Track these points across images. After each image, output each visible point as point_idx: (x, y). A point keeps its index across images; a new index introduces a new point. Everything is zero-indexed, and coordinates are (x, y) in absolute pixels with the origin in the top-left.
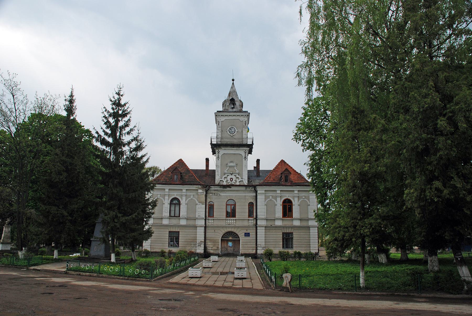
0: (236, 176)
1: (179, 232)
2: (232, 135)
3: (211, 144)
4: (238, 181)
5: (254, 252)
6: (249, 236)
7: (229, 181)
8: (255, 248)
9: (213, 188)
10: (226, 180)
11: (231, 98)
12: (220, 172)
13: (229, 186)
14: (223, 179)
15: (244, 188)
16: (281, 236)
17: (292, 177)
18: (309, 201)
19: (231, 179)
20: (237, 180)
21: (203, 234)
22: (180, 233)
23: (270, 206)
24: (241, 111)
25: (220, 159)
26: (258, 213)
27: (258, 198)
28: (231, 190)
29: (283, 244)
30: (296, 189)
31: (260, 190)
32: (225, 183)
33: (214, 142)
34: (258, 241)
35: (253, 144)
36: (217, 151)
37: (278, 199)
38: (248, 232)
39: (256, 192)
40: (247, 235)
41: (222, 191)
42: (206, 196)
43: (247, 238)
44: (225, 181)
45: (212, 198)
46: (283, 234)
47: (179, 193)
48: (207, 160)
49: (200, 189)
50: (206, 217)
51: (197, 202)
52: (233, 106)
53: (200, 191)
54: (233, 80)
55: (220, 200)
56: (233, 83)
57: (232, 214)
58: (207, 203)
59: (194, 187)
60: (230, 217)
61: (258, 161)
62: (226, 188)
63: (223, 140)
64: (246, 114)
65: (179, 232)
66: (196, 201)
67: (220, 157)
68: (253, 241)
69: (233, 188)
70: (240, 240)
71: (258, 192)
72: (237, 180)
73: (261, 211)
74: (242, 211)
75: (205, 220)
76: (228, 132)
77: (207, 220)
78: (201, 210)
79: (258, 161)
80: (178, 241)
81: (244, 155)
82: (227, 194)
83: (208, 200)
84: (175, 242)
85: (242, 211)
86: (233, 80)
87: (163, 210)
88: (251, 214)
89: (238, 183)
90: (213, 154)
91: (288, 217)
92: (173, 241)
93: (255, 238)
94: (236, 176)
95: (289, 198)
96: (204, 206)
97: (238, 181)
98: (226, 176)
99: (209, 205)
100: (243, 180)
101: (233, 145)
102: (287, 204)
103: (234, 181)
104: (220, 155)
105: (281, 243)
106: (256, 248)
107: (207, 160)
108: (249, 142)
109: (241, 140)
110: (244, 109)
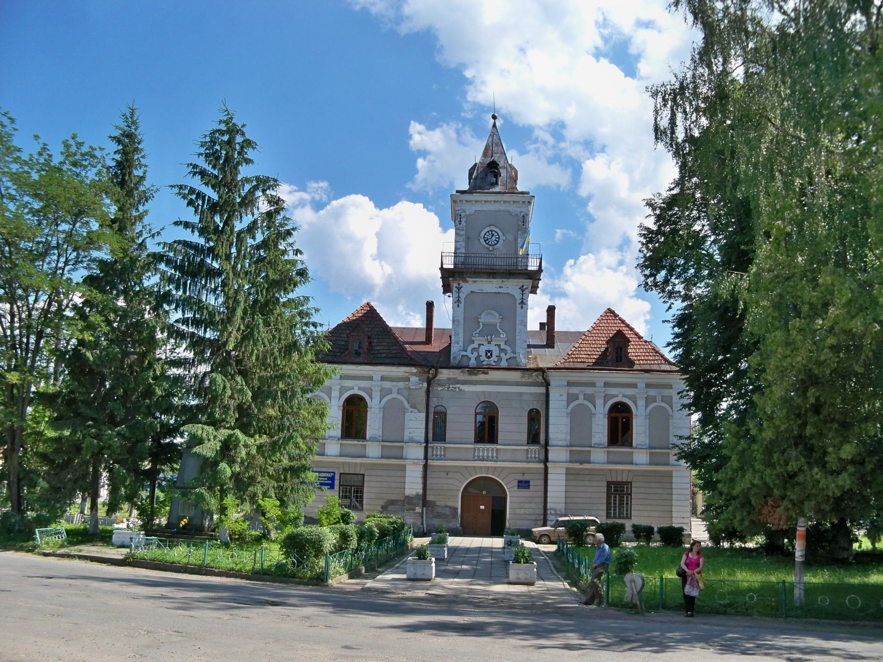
0: (499, 346)
1: (363, 475)
2: (491, 248)
3: (442, 269)
6: (528, 487)
7: (483, 358)
8: (542, 517)
9: (445, 374)
10: (476, 354)
11: (489, 160)
12: (461, 335)
14: (469, 353)
15: (515, 376)
16: (605, 489)
17: (632, 351)
20: (502, 355)
21: (421, 481)
23: (579, 420)
24: (513, 191)
25: (462, 305)
26: (551, 435)
27: (551, 398)
29: (608, 509)
32: (473, 363)
33: (449, 264)
34: (549, 500)
35: (540, 270)
36: (454, 285)
37: (599, 402)
38: (526, 478)
39: (547, 384)
40: (524, 484)
41: (465, 383)
42: (428, 392)
43: (524, 493)
44: (473, 357)
46: (609, 484)
48: (430, 306)
50: (427, 441)
51: (407, 405)
52: (494, 180)
53: (414, 379)
58: (432, 410)
61: (551, 310)
62: (476, 374)
63: (470, 261)
64: (525, 198)
65: (363, 475)
66: (406, 403)
67: (462, 300)
68: (538, 500)
69: (494, 375)
70: (506, 498)
72: (502, 355)
73: (559, 428)
74: (513, 427)
75: (426, 448)
76: (482, 240)
77: (430, 450)
78: (415, 424)
79: (551, 310)
80: (362, 497)
81: (518, 296)
82: (477, 390)
83: (434, 402)
84: (354, 499)
85: (513, 427)
88: (533, 438)
89: (504, 364)
90: (444, 292)
91: (623, 445)
92: (350, 498)
93: (542, 494)
96: (423, 415)
98: (475, 345)
99: (435, 413)
100: (517, 355)
101: (492, 273)
102: (620, 415)
103: (494, 358)
105: (604, 507)
106: (545, 514)
107: (430, 306)
108: (533, 266)
109: (512, 261)
110: (520, 187)
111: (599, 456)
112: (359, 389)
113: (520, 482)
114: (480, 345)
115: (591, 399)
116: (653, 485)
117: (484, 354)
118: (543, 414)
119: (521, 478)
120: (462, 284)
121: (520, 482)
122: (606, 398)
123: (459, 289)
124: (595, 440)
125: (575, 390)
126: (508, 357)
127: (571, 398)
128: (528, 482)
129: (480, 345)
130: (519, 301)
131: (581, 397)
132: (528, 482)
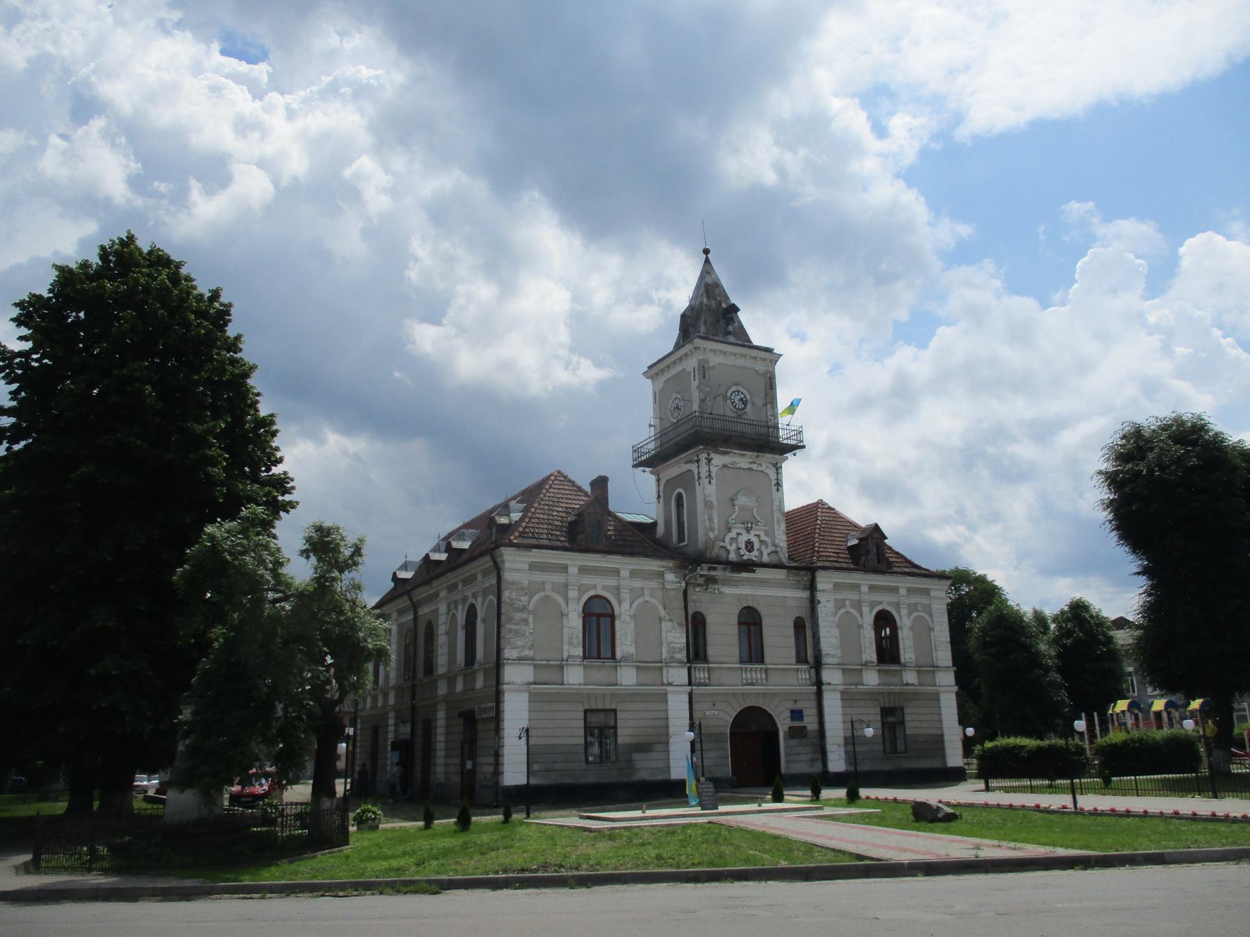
1: (615, 711)
4: (766, 552)
5: (818, 768)
13: (748, 566)
14: (727, 544)
15: (780, 574)
18: (931, 616)
19: (749, 546)
20: (763, 548)
22: (619, 715)
23: (848, 628)
25: (713, 482)
28: (749, 580)
30: (904, 583)
31: (825, 581)
32: (733, 557)
38: (798, 706)
39: (812, 587)
41: (727, 582)
44: (732, 548)
45: (701, 600)
47: (612, 582)
49: (670, 570)
50: (689, 661)
51: (663, 613)
53: (670, 577)
54: (706, 252)
55: (722, 605)
56: (707, 261)
57: (753, 652)
59: (653, 565)
60: (750, 661)
62: (739, 571)
65: (615, 711)
67: (713, 475)
71: (820, 586)
72: (763, 548)
74: (778, 640)
86: (706, 252)
87: (566, 638)
89: (766, 559)
94: (758, 536)
95: (888, 608)
97: (766, 552)
103: (755, 553)
104: (714, 470)
111: (871, 679)
112: (604, 588)
113: (793, 712)
114: (738, 534)
115: (858, 605)
116: (923, 711)
117: (743, 546)
118: (808, 624)
119: (791, 705)
120: (712, 455)
121: (793, 712)
122: (582, 589)
123: (709, 461)
124: (866, 657)
125: (842, 596)
126: (769, 550)
127: (840, 604)
128: (800, 712)
129: (738, 534)
130: (774, 482)
131: (548, 586)
132: (800, 712)
